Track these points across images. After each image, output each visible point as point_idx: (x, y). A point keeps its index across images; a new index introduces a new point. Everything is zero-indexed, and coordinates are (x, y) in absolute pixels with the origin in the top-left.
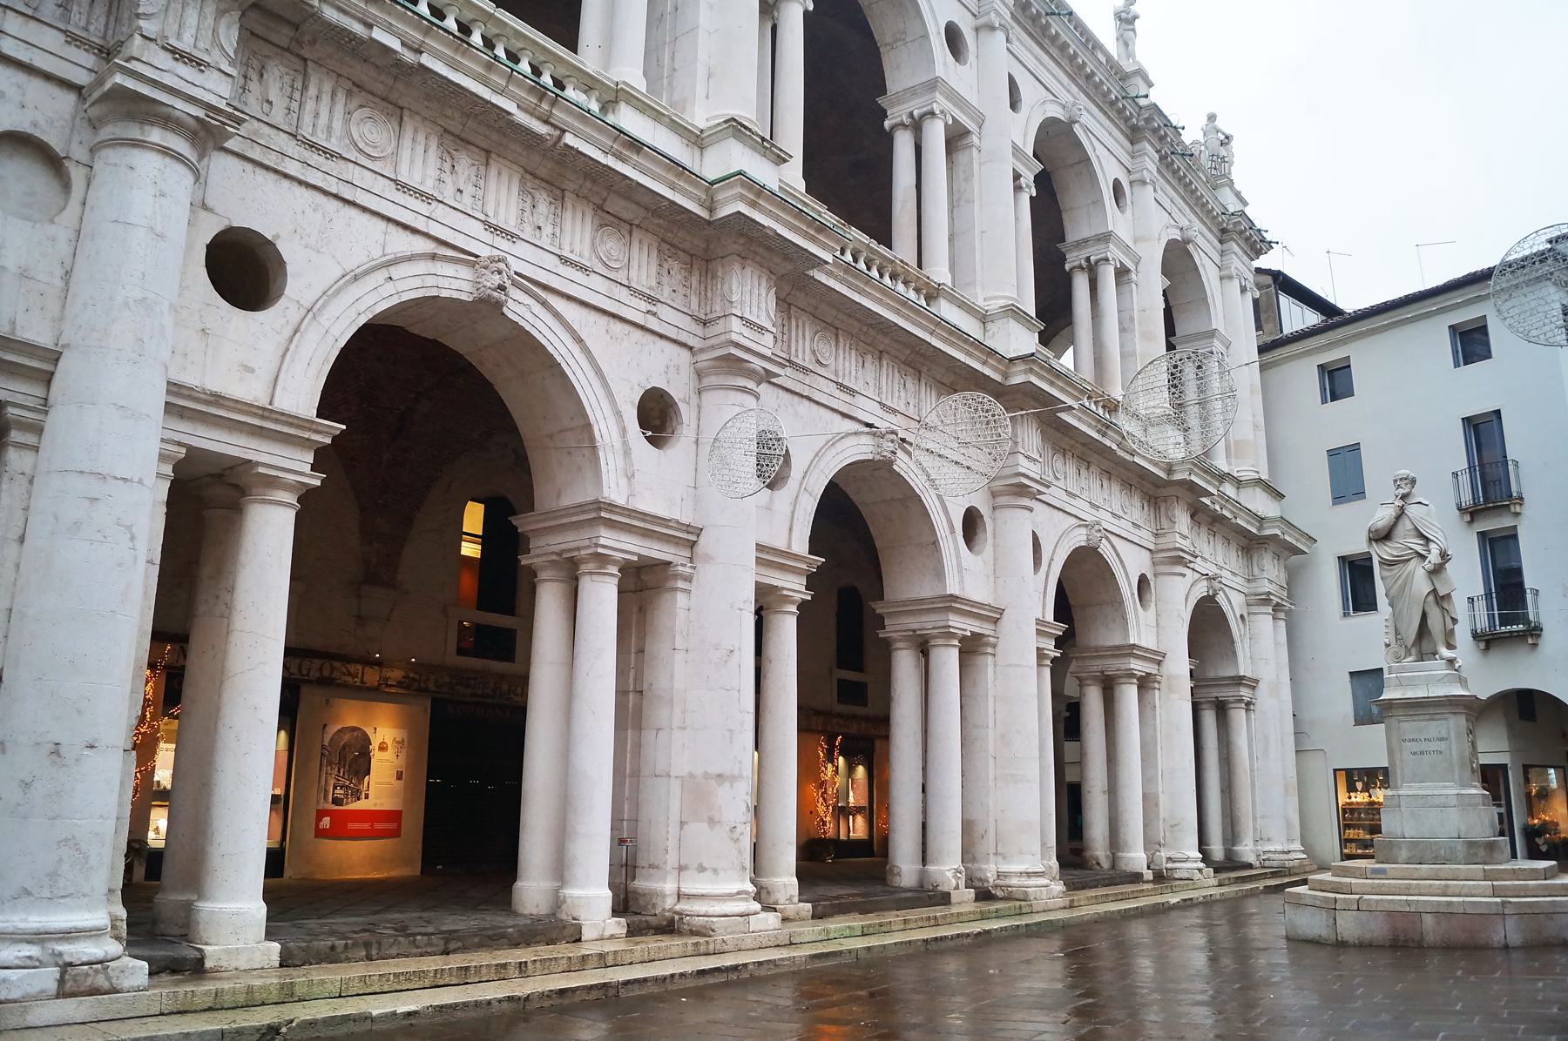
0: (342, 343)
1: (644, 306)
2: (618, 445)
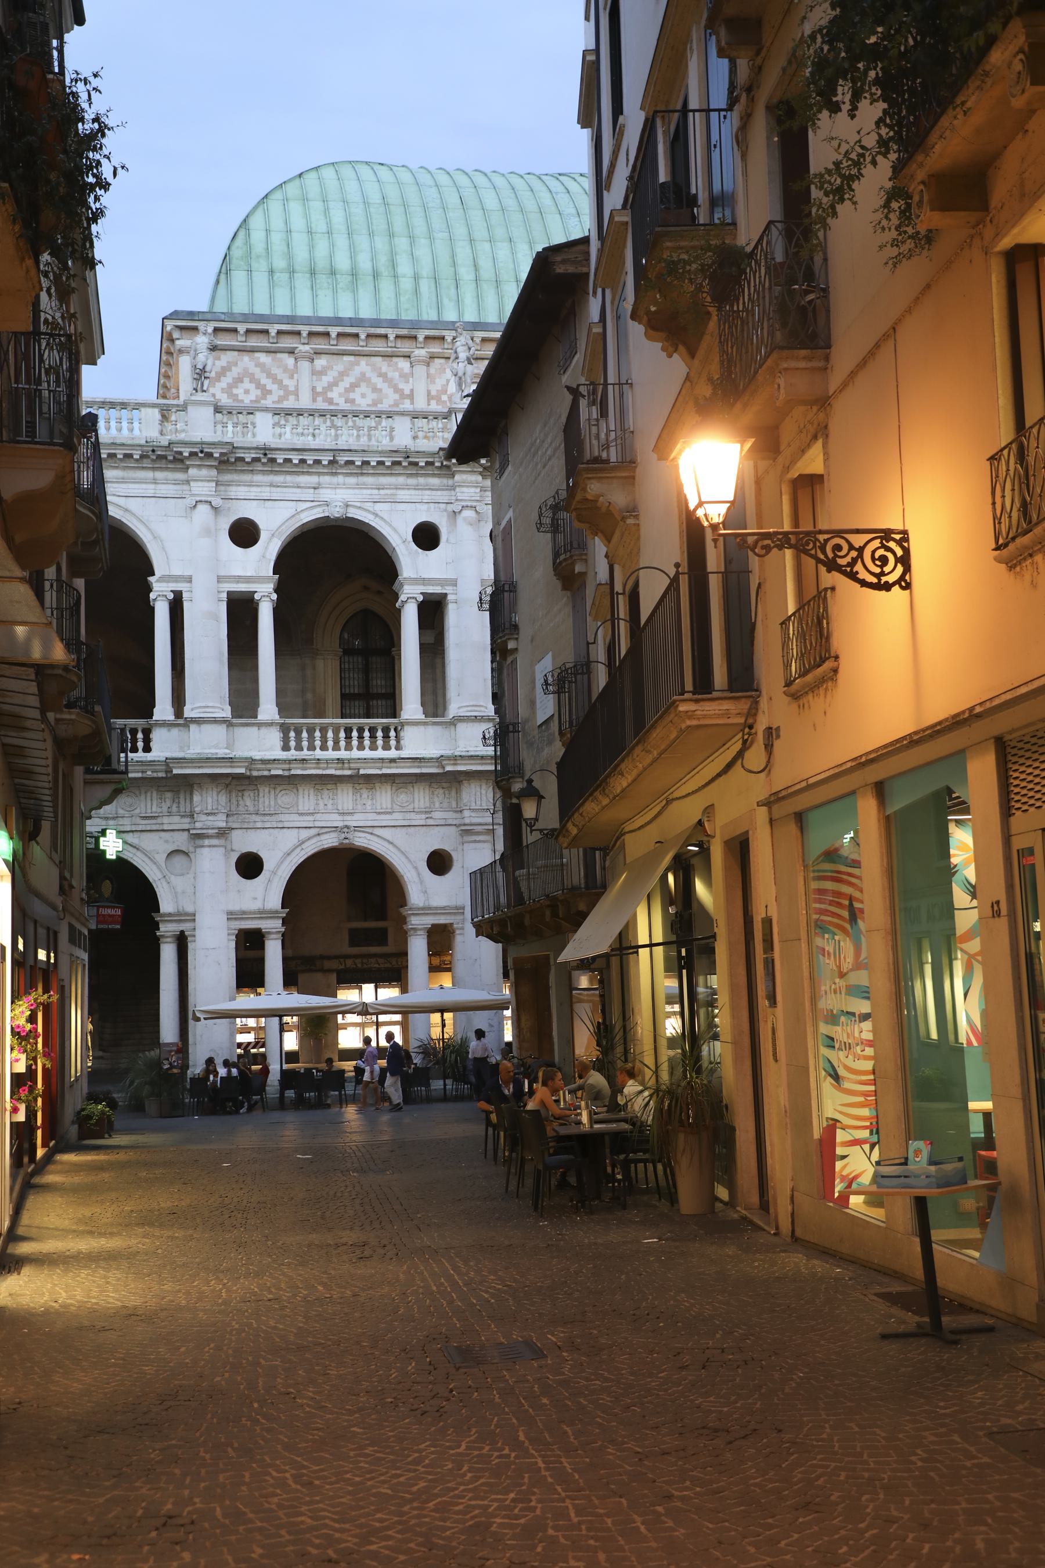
1: (424, 816)
2: (417, 880)
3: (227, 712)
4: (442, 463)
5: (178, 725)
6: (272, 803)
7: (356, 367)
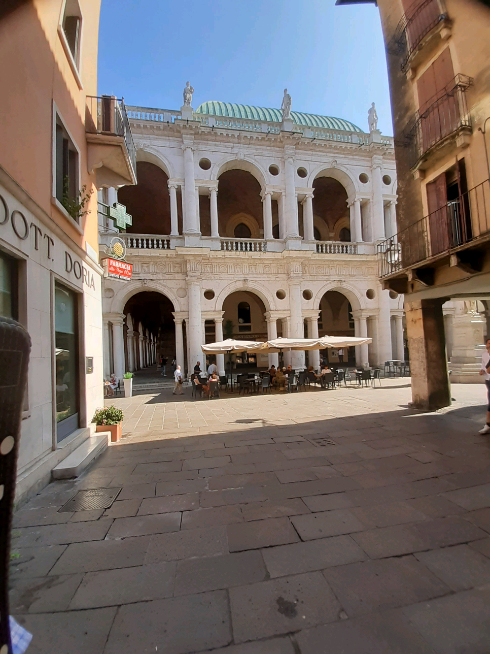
5: (181, 238)
6: (218, 270)
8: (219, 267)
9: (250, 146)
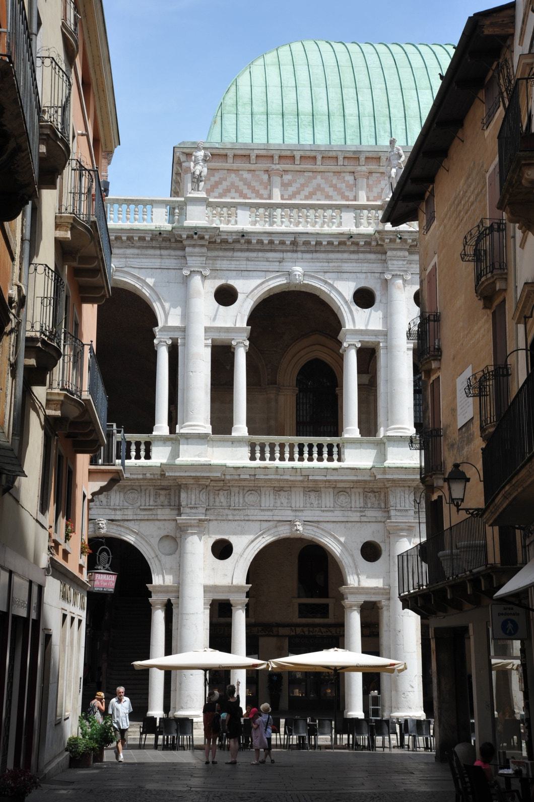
0: (251, 560)
1: (359, 514)
2: (352, 565)
3: (208, 429)
4: (377, 242)
5: (171, 439)
6: (241, 501)
7: (314, 181)
8: (244, 497)
9: (315, 255)
